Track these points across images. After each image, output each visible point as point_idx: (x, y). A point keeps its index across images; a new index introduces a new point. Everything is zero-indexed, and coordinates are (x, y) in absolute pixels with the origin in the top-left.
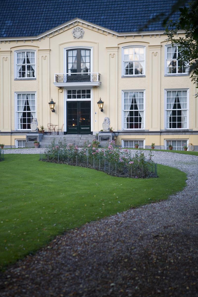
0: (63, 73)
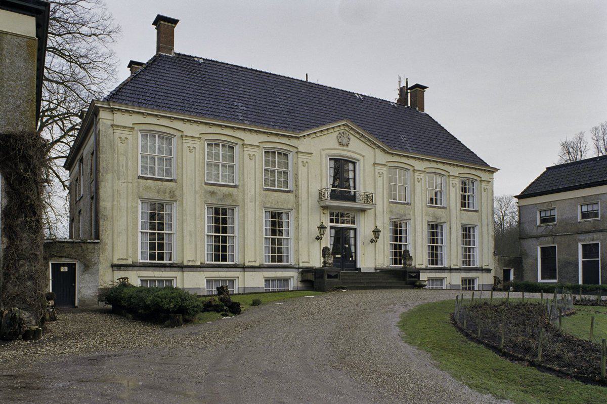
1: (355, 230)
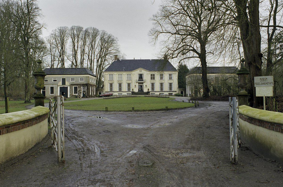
0: (138, 79)
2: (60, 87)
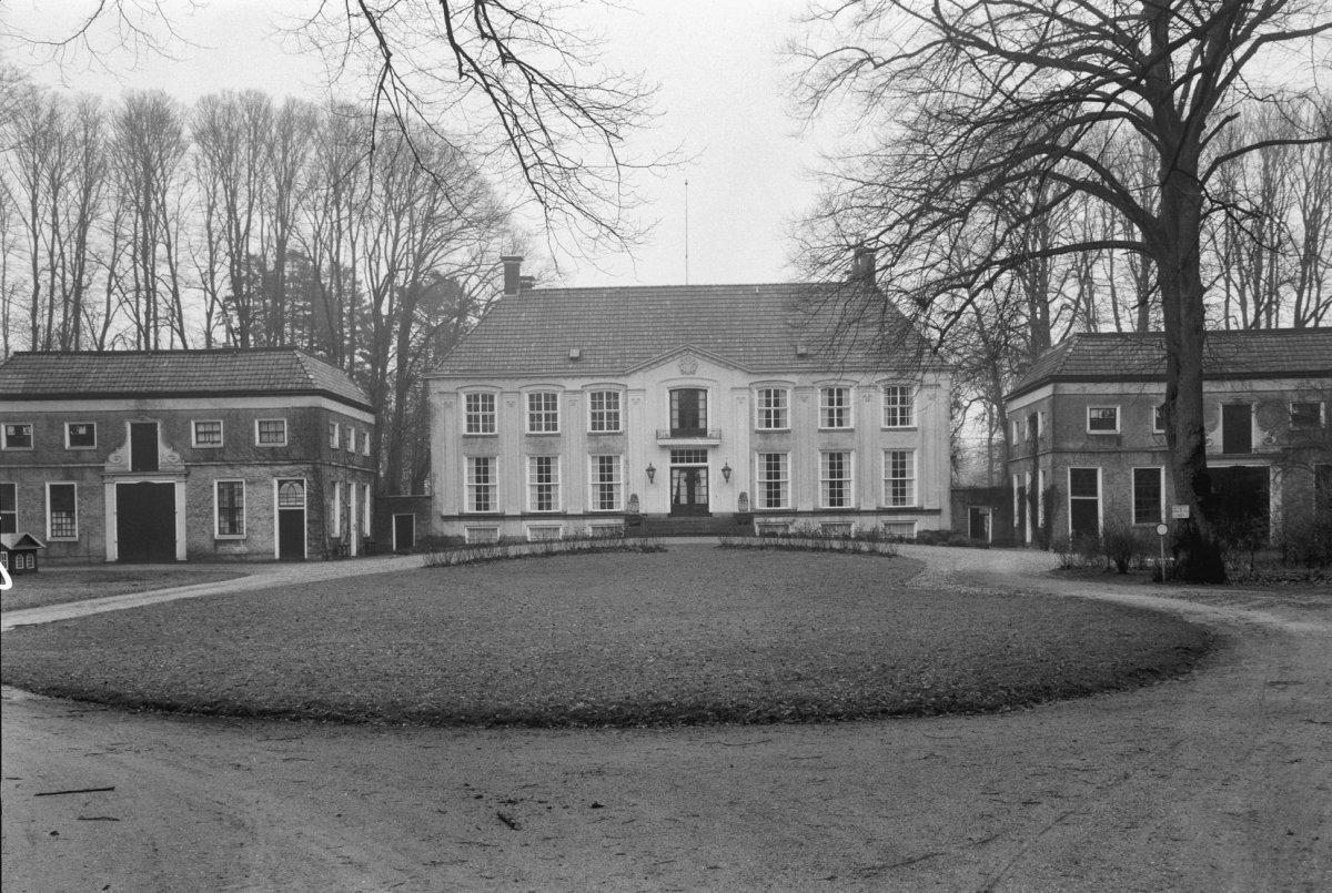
1: (706, 468)
2: (119, 487)
